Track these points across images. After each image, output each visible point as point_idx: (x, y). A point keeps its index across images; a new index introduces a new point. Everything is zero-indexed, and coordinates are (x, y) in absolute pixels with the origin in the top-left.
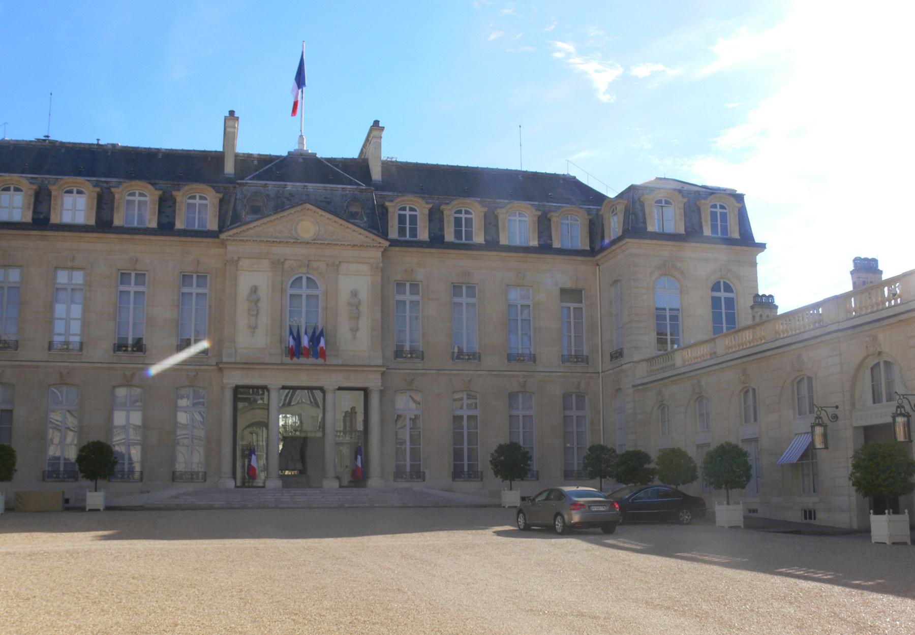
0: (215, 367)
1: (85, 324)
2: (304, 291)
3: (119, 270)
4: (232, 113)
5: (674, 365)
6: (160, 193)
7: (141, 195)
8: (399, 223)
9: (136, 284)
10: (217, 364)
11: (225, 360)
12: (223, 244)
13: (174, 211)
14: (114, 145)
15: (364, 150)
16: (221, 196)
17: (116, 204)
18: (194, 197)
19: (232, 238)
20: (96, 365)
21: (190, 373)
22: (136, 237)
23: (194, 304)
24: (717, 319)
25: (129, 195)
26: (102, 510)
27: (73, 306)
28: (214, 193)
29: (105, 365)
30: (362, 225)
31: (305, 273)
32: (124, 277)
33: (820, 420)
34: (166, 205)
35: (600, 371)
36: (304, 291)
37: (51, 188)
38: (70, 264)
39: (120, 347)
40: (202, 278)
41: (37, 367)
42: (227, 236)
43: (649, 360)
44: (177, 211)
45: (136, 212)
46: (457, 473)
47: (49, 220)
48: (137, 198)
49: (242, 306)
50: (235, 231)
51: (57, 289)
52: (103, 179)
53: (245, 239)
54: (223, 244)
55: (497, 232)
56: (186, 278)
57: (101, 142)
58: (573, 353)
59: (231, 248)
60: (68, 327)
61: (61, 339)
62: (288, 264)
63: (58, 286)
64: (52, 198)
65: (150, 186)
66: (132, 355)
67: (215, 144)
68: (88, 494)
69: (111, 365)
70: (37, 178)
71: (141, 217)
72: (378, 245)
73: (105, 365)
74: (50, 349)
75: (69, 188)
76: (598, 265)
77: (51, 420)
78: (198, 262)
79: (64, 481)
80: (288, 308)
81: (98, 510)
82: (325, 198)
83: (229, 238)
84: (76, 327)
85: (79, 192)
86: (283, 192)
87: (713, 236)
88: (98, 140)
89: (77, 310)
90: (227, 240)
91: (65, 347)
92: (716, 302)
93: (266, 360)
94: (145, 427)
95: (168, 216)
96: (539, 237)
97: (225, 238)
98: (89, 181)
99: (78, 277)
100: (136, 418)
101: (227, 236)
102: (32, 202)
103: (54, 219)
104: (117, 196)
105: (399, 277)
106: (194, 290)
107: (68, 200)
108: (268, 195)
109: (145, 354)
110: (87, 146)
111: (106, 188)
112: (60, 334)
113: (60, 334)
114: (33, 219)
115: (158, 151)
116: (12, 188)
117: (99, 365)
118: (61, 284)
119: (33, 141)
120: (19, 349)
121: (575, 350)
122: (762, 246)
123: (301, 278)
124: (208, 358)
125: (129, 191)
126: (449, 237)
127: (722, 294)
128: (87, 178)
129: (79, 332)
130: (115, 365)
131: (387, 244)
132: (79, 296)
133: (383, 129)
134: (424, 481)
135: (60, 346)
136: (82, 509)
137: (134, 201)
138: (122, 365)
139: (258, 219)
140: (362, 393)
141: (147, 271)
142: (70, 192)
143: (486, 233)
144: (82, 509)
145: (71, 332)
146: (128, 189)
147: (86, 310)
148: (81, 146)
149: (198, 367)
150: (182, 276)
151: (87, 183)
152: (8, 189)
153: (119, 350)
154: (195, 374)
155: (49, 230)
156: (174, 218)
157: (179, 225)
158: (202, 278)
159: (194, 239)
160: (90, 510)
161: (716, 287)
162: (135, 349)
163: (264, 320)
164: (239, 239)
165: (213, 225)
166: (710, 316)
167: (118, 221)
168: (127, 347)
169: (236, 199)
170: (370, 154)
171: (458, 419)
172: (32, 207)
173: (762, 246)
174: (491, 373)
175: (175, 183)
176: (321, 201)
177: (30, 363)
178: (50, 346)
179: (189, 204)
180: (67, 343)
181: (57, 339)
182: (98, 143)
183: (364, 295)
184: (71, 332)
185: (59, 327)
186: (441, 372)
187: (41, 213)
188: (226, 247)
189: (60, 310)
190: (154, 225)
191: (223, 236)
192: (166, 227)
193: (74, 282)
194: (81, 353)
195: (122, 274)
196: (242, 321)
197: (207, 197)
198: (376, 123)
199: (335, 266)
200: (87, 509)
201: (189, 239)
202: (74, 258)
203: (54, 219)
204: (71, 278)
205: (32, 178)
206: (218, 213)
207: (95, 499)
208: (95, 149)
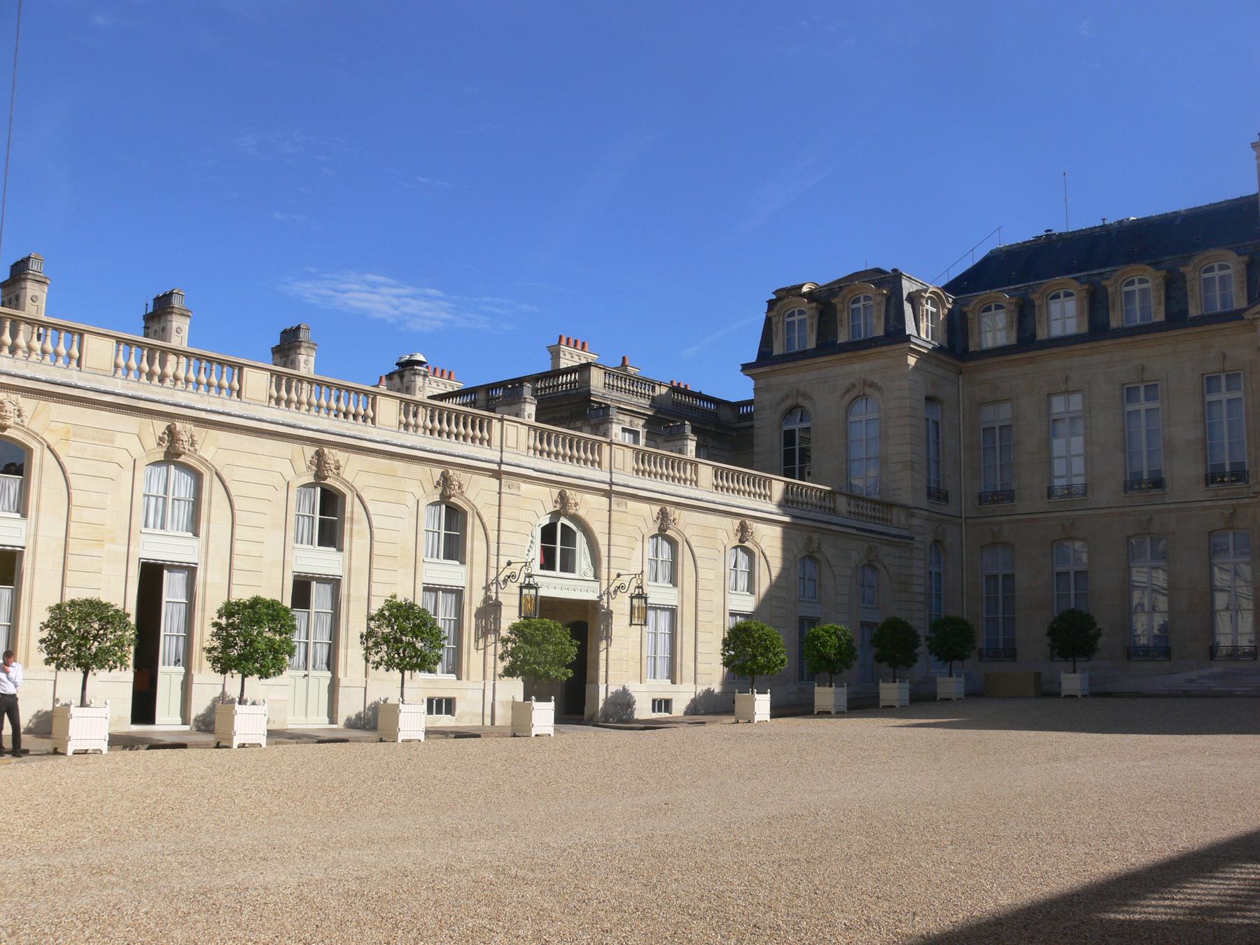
1: (1089, 459)
3: (1123, 385)
6: (1163, 273)
7: (1142, 281)
9: (1147, 399)
13: (1186, 294)
14: (1120, 222)
16: (1246, 258)
17: (1110, 301)
18: (1211, 269)
20: (1104, 511)
21: (1224, 511)
22: (1138, 338)
23: (1225, 414)
25: (1127, 285)
26: (1079, 696)
27: (1073, 439)
28: (1235, 255)
29: (1114, 510)
32: (1130, 393)
33: (640, 590)
34: (1174, 288)
37: (1033, 297)
38: (1063, 388)
39: (1132, 484)
40: (1232, 377)
41: (1036, 520)
42: (1254, 314)
44: (1189, 293)
45: (1218, 293)
48: (1137, 287)
51: (1055, 420)
52: (1096, 272)
56: (1210, 382)
57: (1107, 222)
60: (1069, 466)
61: (1063, 482)
63: (1054, 417)
64: (1036, 309)
65: (1150, 269)
66: (1147, 494)
68: (1063, 676)
69: (1122, 509)
70: (1020, 287)
71: (1223, 298)
73: (1114, 510)
74: (1049, 496)
75: (1054, 293)
77: (1135, 584)
78: (1224, 356)
79: (1154, 660)
81: (1076, 696)
83: (1256, 316)
84: (1078, 466)
85: (1068, 295)
88: (1104, 220)
89: (1078, 444)
90: (1254, 319)
91: (1066, 492)
94: (1171, 590)
97: (1251, 317)
98: (1074, 278)
99: (1076, 402)
100: (1161, 578)
101: (1254, 314)
103: (1041, 335)
104: (1110, 290)
106: (1223, 396)
107: (1055, 306)
109: (1164, 491)
110: (1088, 232)
112: (1060, 477)
113: (1060, 477)
114: (1019, 339)
115: (1176, 214)
116: (993, 307)
117: (1108, 511)
118: (1058, 413)
119: (1030, 241)
120: (1015, 501)
124: (1248, 487)
125: (1124, 280)
128: (1071, 276)
129: (1082, 471)
130: (1127, 509)
132: (1080, 426)
135: (1059, 492)
136: (1057, 695)
137: (1211, 280)
138: (1136, 509)
141: (1158, 380)
142: (1057, 296)
144: (1057, 695)
145: (1074, 472)
146: (1124, 278)
147: (1087, 442)
148: (1081, 233)
149: (1235, 502)
150: (1205, 380)
151: (1073, 281)
152: (988, 309)
153: (1132, 489)
154: (1232, 511)
155: (1033, 350)
156: (1186, 303)
157: (1193, 311)
158: (1232, 377)
159: (1214, 327)
160: (1066, 696)
162: (1150, 486)
165: (1239, 301)
167: (1115, 322)
171: (992, 578)
175: (1186, 255)
177: (1027, 516)
178: (1050, 492)
179: (1127, 293)
180: (1069, 487)
181: (1058, 483)
182: (1104, 224)
184: (1074, 472)
185: (1059, 467)
189: (1058, 446)
190: (1160, 317)
192: (1177, 319)
193: (1072, 408)
194: (1085, 498)
195: (1128, 389)
197: (1230, 265)
200: (1062, 695)
201: (1207, 328)
202: (1067, 379)
203: (1041, 335)
204: (1068, 403)
205: (1014, 289)
206: (1245, 284)
207: (1072, 682)
208: (1098, 234)
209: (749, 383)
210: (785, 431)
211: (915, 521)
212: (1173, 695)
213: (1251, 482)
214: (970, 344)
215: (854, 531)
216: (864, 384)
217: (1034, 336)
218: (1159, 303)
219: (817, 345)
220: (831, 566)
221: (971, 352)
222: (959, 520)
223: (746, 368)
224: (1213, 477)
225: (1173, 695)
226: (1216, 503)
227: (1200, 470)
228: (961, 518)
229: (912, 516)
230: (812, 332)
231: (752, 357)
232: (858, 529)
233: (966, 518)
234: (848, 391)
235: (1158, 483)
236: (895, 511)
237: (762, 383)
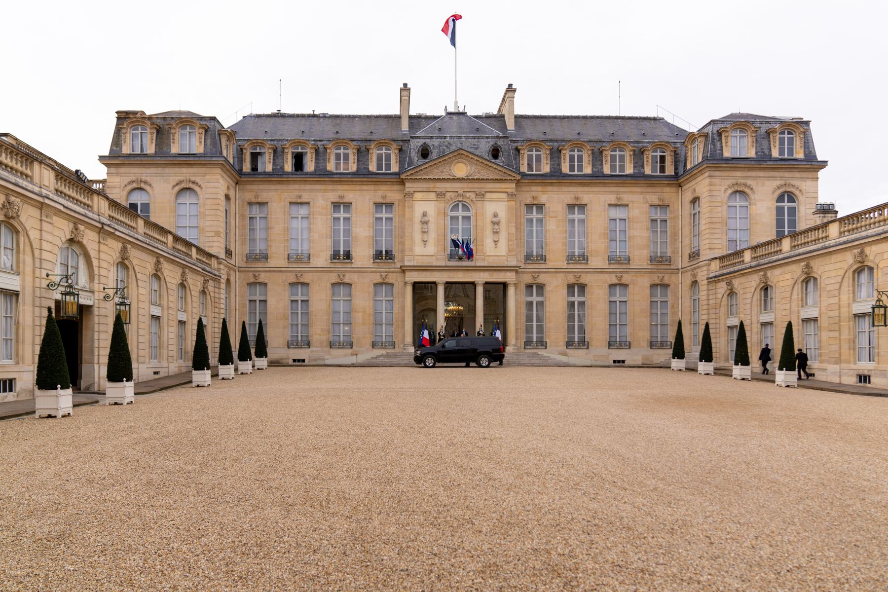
0: (400, 270)
2: (460, 213)
4: (405, 85)
5: (743, 261)
8: (528, 161)
10: (401, 267)
11: (406, 264)
12: (402, 182)
15: (502, 108)
19: (409, 177)
24: (780, 223)
30: (501, 164)
31: (460, 201)
35: (680, 268)
36: (460, 213)
39: (335, 256)
43: (721, 258)
46: (570, 344)
47: (284, 169)
49: (417, 227)
50: (411, 172)
53: (418, 178)
54: (402, 182)
55: (602, 164)
58: (659, 255)
59: (407, 185)
62: (448, 195)
67: (395, 110)
69: (329, 269)
72: (513, 178)
76: (680, 186)
80: (449, 227)
82: (474, 145)
86: (444, 142)
87: (780, 157)
92: (780, 211)
93: (435, 264)
95: (364, 164)
96: (635, 167)
97: (404, 178)
102: (272, 158)
105: (528, 202)
108: (433, 145)
111: (321, 145)
114: (273, 169)
117: (322, 269)
121: (661, 252)
122: (824, 164)
123: (458, 204)
126: (565, 169)
127: (786, 204)
130: (332, 269)
131: (518, 177)
133: (515, 90)
134: (546, 348)
138: (337, 269)
139: (426, 163)
140: (502, 285)
143: (593, 166)
149: (388, 270)
161: (780, 199)
163: (432, 236)
164: (413, 177)
166: (775, 222)
168: (340, 256)
169: (410, 149)
170: (505, 112)
172: (272, 161)
173: (824, 164)
174: (596, 270)
176: (471, 148)
183: (503, 215)
186: (558, 270)
187: (279, 165)
188: (405, 185)
191: (403, 176)
196: (418, 237)
198: (510, 85)
199: (481, 195)
209: (105, 169)
210: (130, 203)
211: (222, 267)
212: (353, 366)
213: (396, 261)
214: (243, 168)
215: (200, 270)
216: (189, 181)
217: (282, 168)
218: (354, 163)
219: (155, 152)
220: (190, 290)
221: (245, 172)
222: (235, 268)
223: (102, 158)
224: (378, 255)
225: (353, 366)
226: (378, 270)
227: (371, 252)
228: (236, 266)
229: (220, 264)
230: (152, 143)
231: (107, 153)
232: (203, 269)
233: (239, 267)
234: (177, 184)
235: (348, 256)
236: (213, 259)
237: (113, 170)
